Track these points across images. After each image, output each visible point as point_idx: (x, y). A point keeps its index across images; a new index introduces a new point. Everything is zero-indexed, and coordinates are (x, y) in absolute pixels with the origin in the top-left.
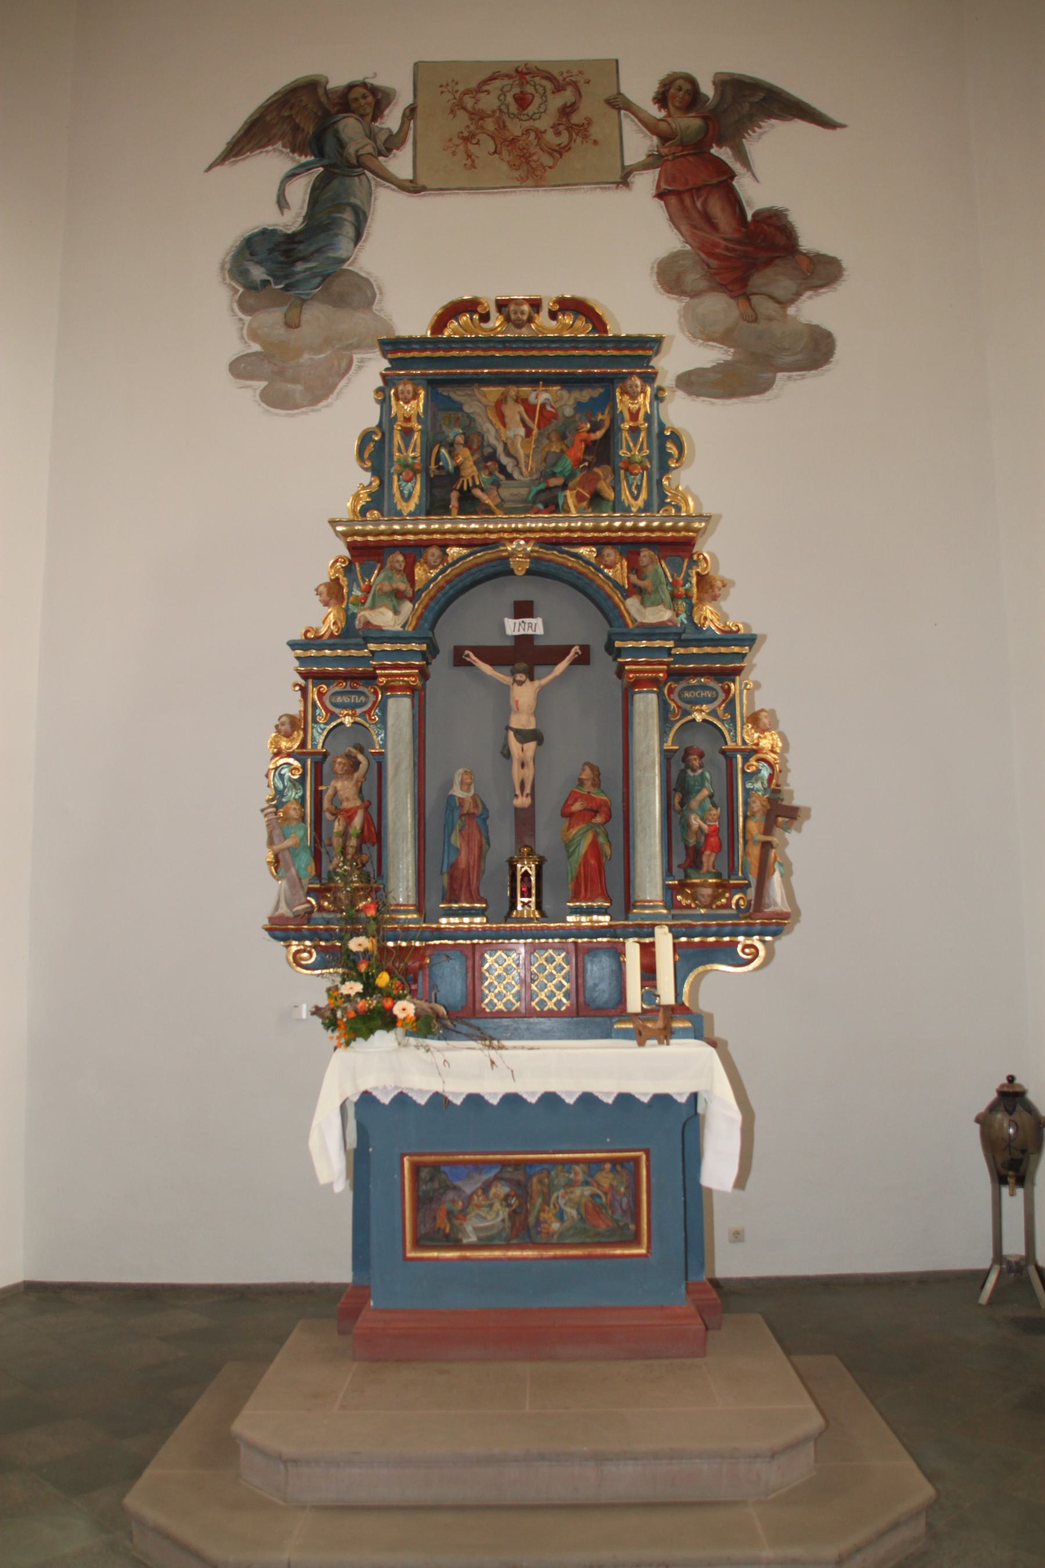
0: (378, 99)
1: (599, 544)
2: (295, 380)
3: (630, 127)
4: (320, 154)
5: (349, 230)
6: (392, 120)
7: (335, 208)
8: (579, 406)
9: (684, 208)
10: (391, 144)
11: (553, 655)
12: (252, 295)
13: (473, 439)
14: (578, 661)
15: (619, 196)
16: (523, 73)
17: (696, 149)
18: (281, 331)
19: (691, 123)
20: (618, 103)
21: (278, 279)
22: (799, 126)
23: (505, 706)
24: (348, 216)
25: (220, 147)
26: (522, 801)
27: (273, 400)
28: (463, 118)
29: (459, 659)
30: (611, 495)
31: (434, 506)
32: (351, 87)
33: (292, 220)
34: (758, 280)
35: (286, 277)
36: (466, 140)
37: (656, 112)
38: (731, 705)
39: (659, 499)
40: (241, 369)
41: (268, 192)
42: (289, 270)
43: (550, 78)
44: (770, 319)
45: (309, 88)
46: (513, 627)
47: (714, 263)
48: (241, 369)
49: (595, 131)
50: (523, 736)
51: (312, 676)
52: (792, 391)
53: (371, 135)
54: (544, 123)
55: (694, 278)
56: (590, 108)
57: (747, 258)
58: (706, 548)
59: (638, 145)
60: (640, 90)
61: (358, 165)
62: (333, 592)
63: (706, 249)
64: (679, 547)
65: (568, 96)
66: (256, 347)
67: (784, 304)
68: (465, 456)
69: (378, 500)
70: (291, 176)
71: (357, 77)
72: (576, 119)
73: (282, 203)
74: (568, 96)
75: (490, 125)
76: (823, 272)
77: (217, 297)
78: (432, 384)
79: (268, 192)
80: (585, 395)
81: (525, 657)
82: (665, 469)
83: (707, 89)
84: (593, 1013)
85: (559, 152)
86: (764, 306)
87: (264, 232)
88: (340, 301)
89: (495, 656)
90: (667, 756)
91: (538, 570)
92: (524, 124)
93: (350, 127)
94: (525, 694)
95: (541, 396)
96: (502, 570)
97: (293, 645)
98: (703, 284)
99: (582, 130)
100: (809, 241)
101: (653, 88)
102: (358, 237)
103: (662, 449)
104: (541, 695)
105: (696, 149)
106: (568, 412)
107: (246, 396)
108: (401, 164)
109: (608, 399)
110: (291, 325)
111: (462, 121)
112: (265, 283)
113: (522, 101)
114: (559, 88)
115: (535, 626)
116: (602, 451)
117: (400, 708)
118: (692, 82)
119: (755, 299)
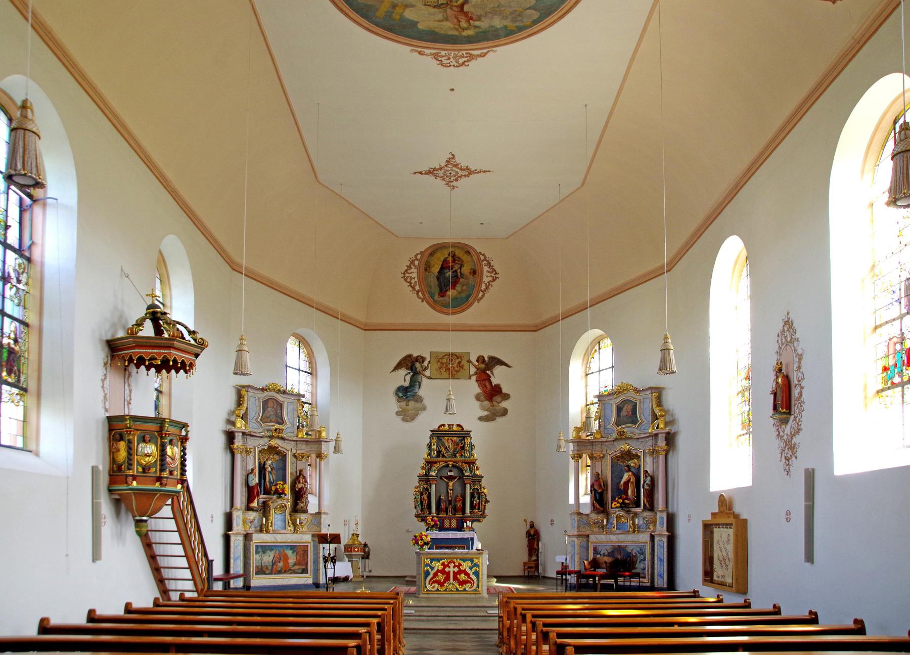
0: (423, 359)
3: (471, 366)
6: (426, 364)
7: (415, 382)
11: (455, 478)
12: (399, 399)
13: (443, 445)
15: (468, 381)
17: (484, 371)
19: (483, 366)
20: (469, 361)
23: (448, 485)
27: (404, 420)
29: (441, 478)
31: (438, 456)
33: (407, 384)
34: (494, 398)
36: (440, 368)
37: (476, 363)
39: (471, 455)
40: (398, 413)
41: (402, 378)
42: (406, 393)
45: (410, 356)
48: (398, 413)
51: (420, 480)
52: (500, 420)
55: (482, 398)
56: (464, 362)
59: (473, 370)
60: (473, 359)
61: (419, 373)
62: (423, 468)
63: (485, 392)
64: (474, 463)
68: (443, 448)
69: (429, 454)
73: (405, 380)
76: (506, 397)
77: (393, 399)
79: (402, 378)
81: (451, 478)
83: (486, 359)
84: (460, 528)
85: (458, 371)
86: (495, 403)
88: (416, 401)
91: (453, 466)
92: (451, 366)
93: (418, 365)
94: (451, 484)
95: (455, 439)
96: (448, 466)
99: (462, 367)
100: (505, 390)
105: (484, 371)
107: (399, 419)
108: (427, 373)
115: (452, 474)
116: (463, 448)
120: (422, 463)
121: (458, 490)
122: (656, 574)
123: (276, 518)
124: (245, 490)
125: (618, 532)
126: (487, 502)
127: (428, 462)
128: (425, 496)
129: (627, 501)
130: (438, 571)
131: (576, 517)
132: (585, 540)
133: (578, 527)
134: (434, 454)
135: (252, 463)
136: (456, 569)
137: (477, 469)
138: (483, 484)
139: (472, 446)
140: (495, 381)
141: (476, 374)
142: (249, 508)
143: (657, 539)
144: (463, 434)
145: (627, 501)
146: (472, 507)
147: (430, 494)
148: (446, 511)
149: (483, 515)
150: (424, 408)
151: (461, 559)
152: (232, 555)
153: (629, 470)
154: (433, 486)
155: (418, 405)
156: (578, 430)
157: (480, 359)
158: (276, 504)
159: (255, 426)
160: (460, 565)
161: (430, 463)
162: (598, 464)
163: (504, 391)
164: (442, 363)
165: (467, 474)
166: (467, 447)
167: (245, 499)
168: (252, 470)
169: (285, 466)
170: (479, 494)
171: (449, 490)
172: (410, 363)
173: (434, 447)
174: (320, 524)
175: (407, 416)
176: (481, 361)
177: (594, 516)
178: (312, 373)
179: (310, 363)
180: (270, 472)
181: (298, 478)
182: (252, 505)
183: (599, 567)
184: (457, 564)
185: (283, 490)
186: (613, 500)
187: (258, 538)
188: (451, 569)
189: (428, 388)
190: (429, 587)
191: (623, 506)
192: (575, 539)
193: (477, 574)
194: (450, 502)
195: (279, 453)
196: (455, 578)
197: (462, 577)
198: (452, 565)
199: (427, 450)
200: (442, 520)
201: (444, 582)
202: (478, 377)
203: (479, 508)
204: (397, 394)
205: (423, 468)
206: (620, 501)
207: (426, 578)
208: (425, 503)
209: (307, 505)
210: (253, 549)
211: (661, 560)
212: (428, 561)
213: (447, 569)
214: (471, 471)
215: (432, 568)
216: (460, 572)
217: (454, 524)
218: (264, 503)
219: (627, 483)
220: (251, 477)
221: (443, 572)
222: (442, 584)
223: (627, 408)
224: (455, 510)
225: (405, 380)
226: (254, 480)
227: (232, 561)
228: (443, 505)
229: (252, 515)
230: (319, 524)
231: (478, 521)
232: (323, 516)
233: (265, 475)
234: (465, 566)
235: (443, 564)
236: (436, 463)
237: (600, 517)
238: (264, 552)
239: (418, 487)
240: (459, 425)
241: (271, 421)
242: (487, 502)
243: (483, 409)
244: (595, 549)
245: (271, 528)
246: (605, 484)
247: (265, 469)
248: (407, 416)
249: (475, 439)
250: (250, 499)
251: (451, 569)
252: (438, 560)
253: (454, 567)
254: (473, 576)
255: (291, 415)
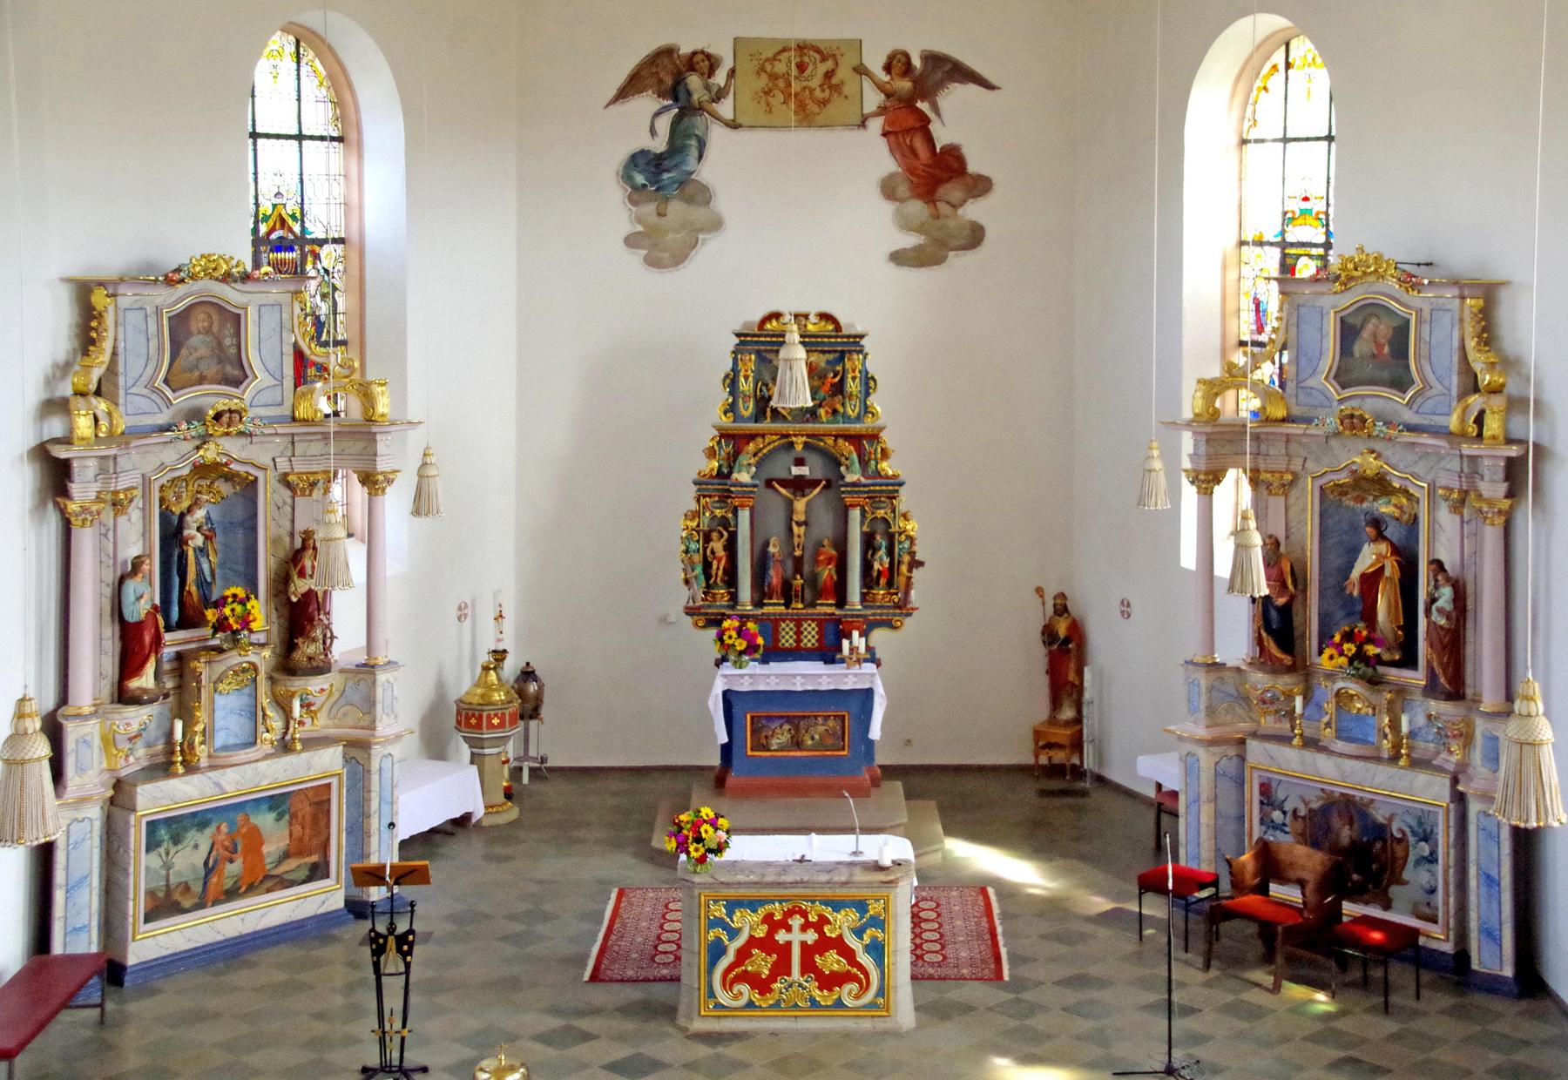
0: (712, 63)
1: (836, 437)
2: (664, 251)
3: (867, 84)
4: (676, 99)
5: (694, 152)
6: (720, 78)
7: (685, 138)
8: (828, 362)
9: (899, 144)
10: (719, 96)
11: (814, 483)
12: (636, 194)
14: (825, 487)
15: (859, 134)
16: (802, 48)
17: (908, 103)
18: (654, 219)
19: (905, 85)
20: (861, 70)
21: (652, 184)
22: (972, 88)
24: (694, 142)
25: (612, 92)
26: (798, 553)
27: (652, 262)
28: (764, 77)
29: (769, 484)
30: (841, 409)
31: (759, 415)
32: (694, 53)
33: (659, 145)
35: (657, 182)
36: (767, 93)
37: (885, 78)
38: (894, 511)
39: (866, 410)
40: (631, 241)
41: (643, 124)
42: (659, 175)
43: (818, 51)
44: (947, 217)
45: (668, 52)
46: (796, 471)
47: (915, 180)
48: (631, 241)
49: (846, 90)
50: (799, 524)
52: (958, 262)
53: (707, 88)
54: (815, 83)
55: (903, 190)
56: (844, 73)
57: (934, 174)
58: (884, 435)
59: (873, 100)
60: (875, 62)
61: (700, 109)
62: (711, 453)
63: (910, 170)
64: (874, 437)
65: (829, 65)
66: (640, 228)
67: (955, 207)
69: (732, 408)
70: (657, 114)
71: (699, 47)
72: (834, 81)
73: (653, 132)
74: (829, 65)
75: (781, 83)
76: (981, 186)
77: (614, 194)
78: (758, 353)
79: (643, 124)
80: (831, 357)
82: (868, 394)
83: (917, 62)
84: (828, 653)
85: (824, 103)
86: (943, 208)
87: (642, 151)
88: (690, 200)
89: (784, 483)
90: (863, 534)
92: (803, 82)
93: (694, 81)
94: (800, 505)
97: (695, 483)
98: (908, 194)
99: (837, 88)
100: (975, 164)
101: (883, 60)
102: (700, 157)
103: (867, 384)
104: (808, 504)
105: (908, 103)
106: (823, 365)
107: (636, 258)
108: (725, 108)
109: (841, 359)
110: (660, 214)
111: (763, 81)
112: (644, 186)
113: (801, 67)
114: (824, 59)
115: (804, 471)
116: (839, 389)
117: (744, 516)
118: (907, 56)
119: (939, 204)
120: (708, 437)
121: (825, 525)
122: (1473, 925)
123: (223, 710)
124: (110, 632)
125: (1340, 746)
126: (915, 564)
127: (725, 435)
128: (718, 546)
129: (1372, 650)
130: (752, 942)
131: (1202, 679)
132: (1232, 751)
133: (1211, 711)
134: (748, 408)
135: (136, 536)
136: (811, 937)
137: (885, 454)
138: (904, 501)
139: (868, 382)
140: (943, 135)
141: (882, 111)
142: (124, 697)
143: (1474, 808)
144: (836, 348)
145: (1372, 650)
146: (869, 580)
147: (731, 547)
148: (788, 593)
149: (903, 607)
150: (716, 225)
151: (826, 903)
152: (59, 876)
153: (1380, 536)
154: (744, 516)
155: (697, 214)
156: (1213, 389)
157: (898, 63)
158: (219, 668)
159: (144, 404)
160: (823, 920)
161: (733, 441)
162: (1276, 503)
163: (973, 167)
164: (773, 77)
165: (851, 478)
166: (852, 386)
167: (110, 666)
168: (137, 564)
169: (255, 515)
170: (891, 538)
171: (793, 517)
172: (672, 77)
173: (745, 386)
174: (373, 704)
175: (662, 250)
176: (898, 66)
177: (1260, 680)
178: (345, 137)
179: (338, 103)
180: (202, 551)
181: (296, 557)
182: (134, 684)
183: (1283, 880)
184: (813, 918)
185: (245, 622)
186: (1325, 638)
187: (155, 799)
188: (796, 937)
189: (728, 159)
190: (724, 998)
191: (1366, 668)
192: (1201, 752)
193: (876, 949)
194: (798, 562)
195: (230, 477)
196: (808, 966)
197: (831, 962)
198: (796, 922)
199: (723, 396)
200: (771, 626)
201: (773, 978)
202: (887, 122)
203: (890, 584)
204: (627, 177)
205: (711, 453)
206: (1349, 648)
207: (713, 962)
208: (718, 568)
209: (327, 650)
210: (137, 836)
211: (1491, 882)
212: (720, 911)
213: (781, 937)
214: (864, 463)
215: (733, 933)
216: (824, 944)
217: (810, 638)
218: (180, 657)
219: (1371, 581)
220: (131, 587)
221: (767, 944)
222: (762, 986)
223: (1379, 328)
224: (819, 593)
225: (653, 132)
226: (142, 598)
227: (59, 896)
228: (774, 577)
229: (136, 717)
230: (369, 704)
231: (889, 624)
232: (382, 677)
233: (183, 557)
234: (842, 923)
235: (768, 919)
236: (752, 437)
237: (1285, 682)
238: (176, 840)
239: (696, 515)
240: (825, 317)
241: (201, 380)
242: (915, 564)
243: (906, 226)
244: (1265, 789)
245: (201, 751)
246: (1299, 577)
247: (184, 542)
248: (662, 250)
249: (877, 358)
250: (129, 664)
251: (796, 937)
252: (753, 905)
253: (804, 928)
254: (865, 959)
255: (271, 344)
